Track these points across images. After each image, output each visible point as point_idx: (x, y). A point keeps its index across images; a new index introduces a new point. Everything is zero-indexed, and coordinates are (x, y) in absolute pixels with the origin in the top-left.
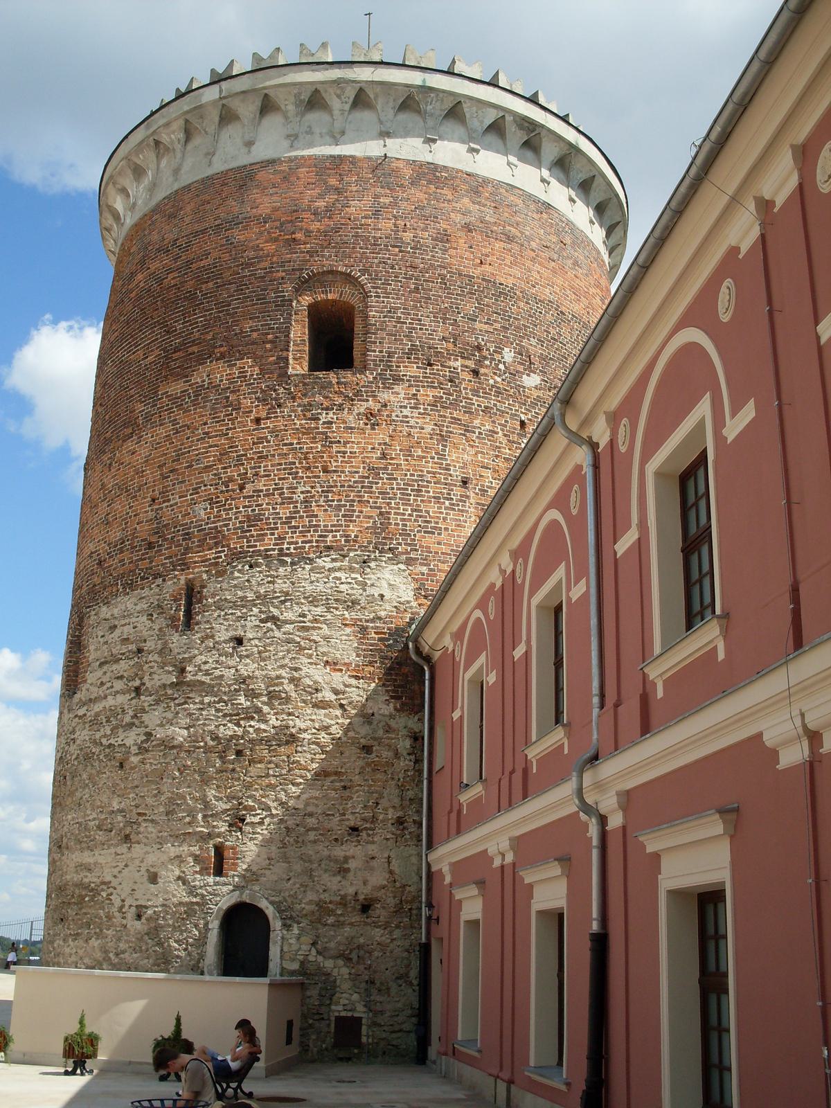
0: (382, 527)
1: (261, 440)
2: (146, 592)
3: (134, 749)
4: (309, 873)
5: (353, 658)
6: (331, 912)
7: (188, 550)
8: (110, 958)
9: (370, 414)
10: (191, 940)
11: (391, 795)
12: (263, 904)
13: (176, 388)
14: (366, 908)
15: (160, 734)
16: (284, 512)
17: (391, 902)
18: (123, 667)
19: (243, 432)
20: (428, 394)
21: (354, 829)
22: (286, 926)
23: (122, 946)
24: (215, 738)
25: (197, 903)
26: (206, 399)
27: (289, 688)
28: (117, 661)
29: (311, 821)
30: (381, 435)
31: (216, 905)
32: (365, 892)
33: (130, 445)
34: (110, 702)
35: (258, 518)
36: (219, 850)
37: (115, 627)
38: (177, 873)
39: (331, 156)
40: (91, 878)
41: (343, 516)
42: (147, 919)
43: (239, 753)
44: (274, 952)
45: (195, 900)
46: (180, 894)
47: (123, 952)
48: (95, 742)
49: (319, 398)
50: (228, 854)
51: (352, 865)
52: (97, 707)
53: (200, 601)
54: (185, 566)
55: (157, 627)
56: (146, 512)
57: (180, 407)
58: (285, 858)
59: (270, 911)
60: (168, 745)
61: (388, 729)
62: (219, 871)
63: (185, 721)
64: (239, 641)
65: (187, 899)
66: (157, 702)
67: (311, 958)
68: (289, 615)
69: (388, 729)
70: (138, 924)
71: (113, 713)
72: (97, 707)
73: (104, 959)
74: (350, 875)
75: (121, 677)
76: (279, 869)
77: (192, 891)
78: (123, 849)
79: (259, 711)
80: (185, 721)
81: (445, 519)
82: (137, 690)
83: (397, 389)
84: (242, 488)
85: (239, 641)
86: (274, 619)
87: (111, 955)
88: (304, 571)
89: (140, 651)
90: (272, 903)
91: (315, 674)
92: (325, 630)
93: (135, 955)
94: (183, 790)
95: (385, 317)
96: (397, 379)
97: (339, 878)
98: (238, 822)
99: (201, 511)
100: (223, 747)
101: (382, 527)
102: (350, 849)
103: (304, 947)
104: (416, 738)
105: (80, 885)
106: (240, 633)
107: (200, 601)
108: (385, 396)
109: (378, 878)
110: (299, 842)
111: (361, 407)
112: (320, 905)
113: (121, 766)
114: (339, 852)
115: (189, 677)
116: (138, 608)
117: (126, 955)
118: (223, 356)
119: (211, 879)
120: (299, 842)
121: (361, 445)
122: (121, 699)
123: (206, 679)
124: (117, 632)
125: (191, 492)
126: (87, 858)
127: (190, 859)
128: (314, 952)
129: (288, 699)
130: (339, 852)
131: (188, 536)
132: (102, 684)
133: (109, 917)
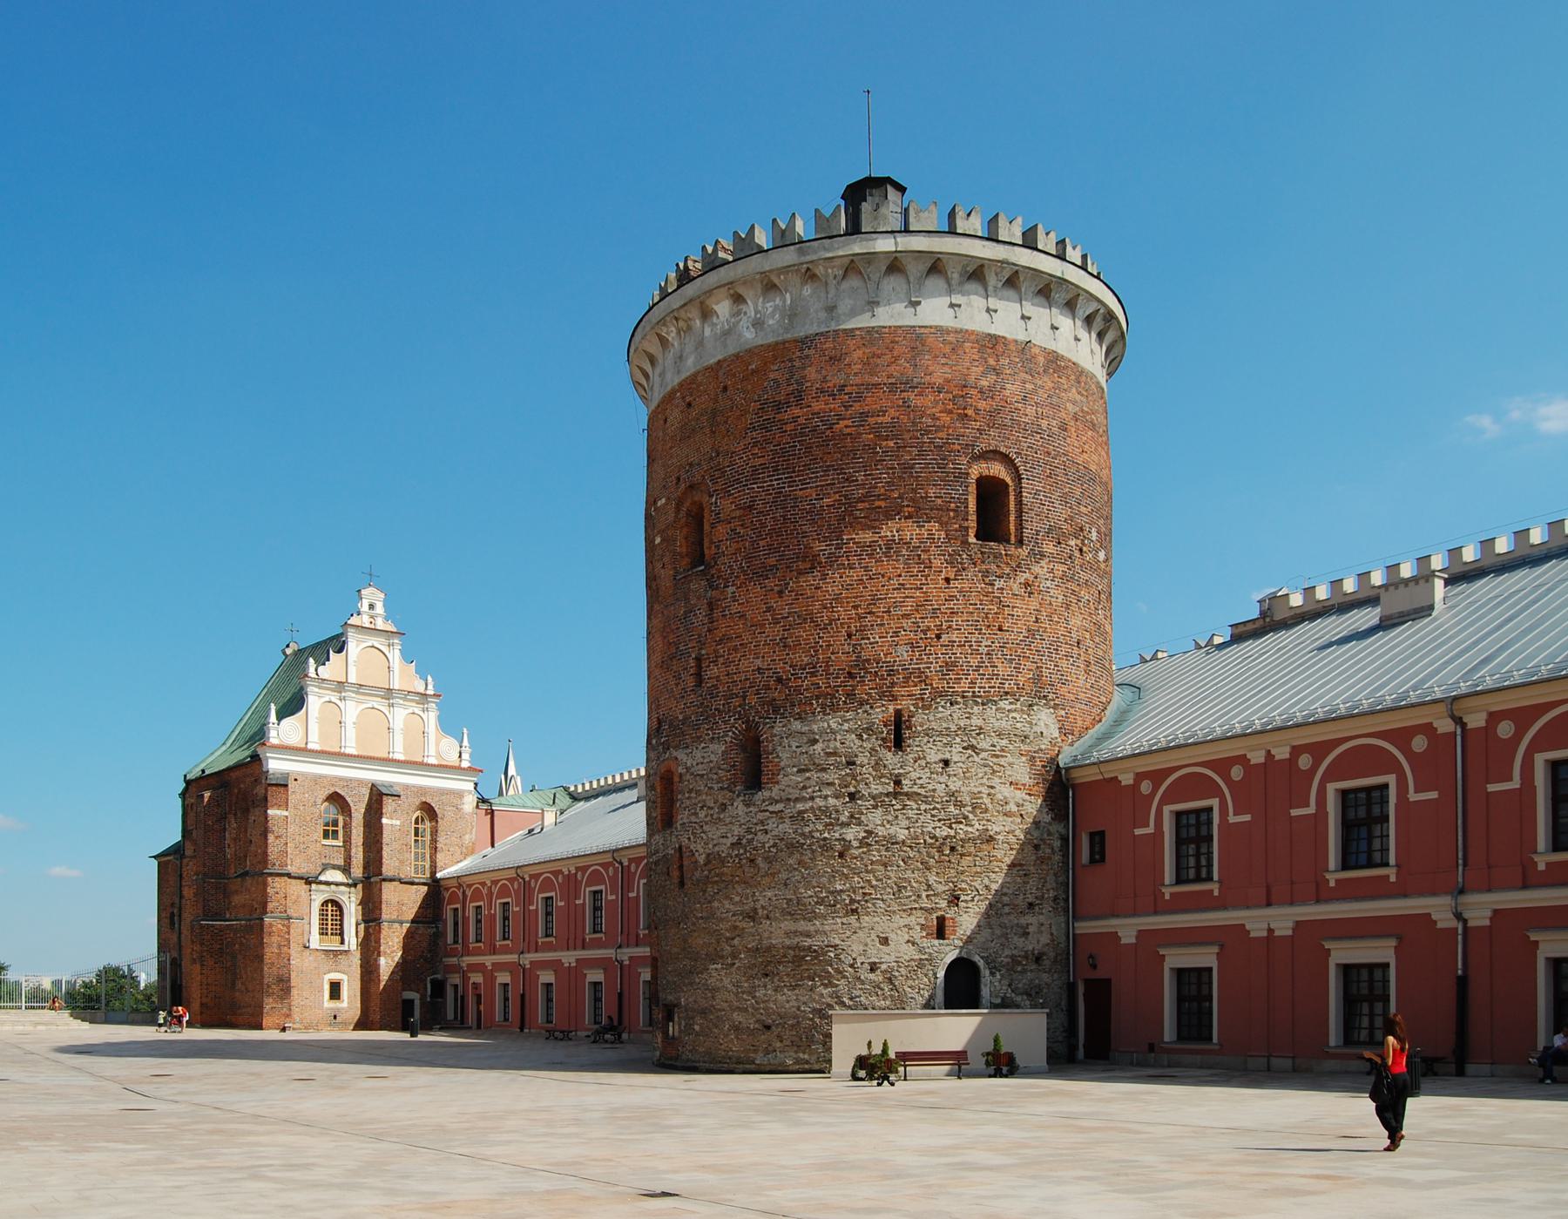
0: (1037, 679)
1: (951, 598)
2: (849, 715)
3: (855, 844)
4: (1005, 936)
5: (1026, 779)
6: (1019, 963)
7: (893, 684)
9: (1027, 584)
11: (1051, 878)
12: (977, 959)
13: (867, 536)
14: (1038, 959)
15: (881, 831)
16: (974, 662)
17: (1052, 955)
18: (831, 776)
19: (935, 588)
20: (1060, 569)
21: (1031, 905)
22: (992, 974)
23: (858, 993)
24: (934, 837)
26: (898, 553)
27: (987, 800)
28: (824, 770)
29: (1006, 899)
30: (1034, 604)
32: (1038, 947)
33: (812, 579)
34: (819, 802)
35: (954, 664)
36: (941, 921)
37: (816, 741)
38: (907, 937)
40: (815, 942)
43: (953, 849)
44: (985, 992)
46: (910, 952)
48: (803, 834)
49: (993, 567)
52: (800, 806)
53: (909, 728)
54: (894, 698)
55: (867, 745)
56: (842, 646)
57: (871, 556)
58: (990, 926)
59: (981, 963)
60: (891, 841)
61: (1049, 834)
62: (941, 933)
63: (905, 823)
64: (946, 763)
66: (875, 807)
68: (984, 745)
69: (1049, 834)
70: (872, 976)
71: (825, 811)
72: (800, 806)
75: (832, 784)
76: (986, 933)
78: (853, 918)
79: (966, 818)
80: (905, 823)
82: (852, 796)
83: (1043, 563)
84: (938, 637)
85: (946, 763)
86: (973, 747)
88: (991, 711)
89: (851, 763)
91: (1005, 791)
92: (1009, 759)
94: (909, 874)
95: (1041, 504)
96: (1043, 555)
98: (955, 900)
99: (903, 653)
100: (940, 844)
101: (1037, 679)
102: (1029, 919)
104: (1065, 839)
105: (797, 947)
106: (947, 756)
107: (909, 728)
108: (1036, 569)
109: (1045, 939)
110: (999, 915)
111: (1023, 577)
112: (1013, 957)
113: (841, 855)
114: (1023, 921)
115: (906, 789)
116: (846, 726)
118: (909, 517)
119: (936, 942)
120: (999, 915)
121: (1024, 608)
122: (832, 801)
123: (922, 791)
124: (818, 747)
126: (803, 926)
129: (986, 811)
131: (891, 673)
132: (805, 788)
133: (838, 971)
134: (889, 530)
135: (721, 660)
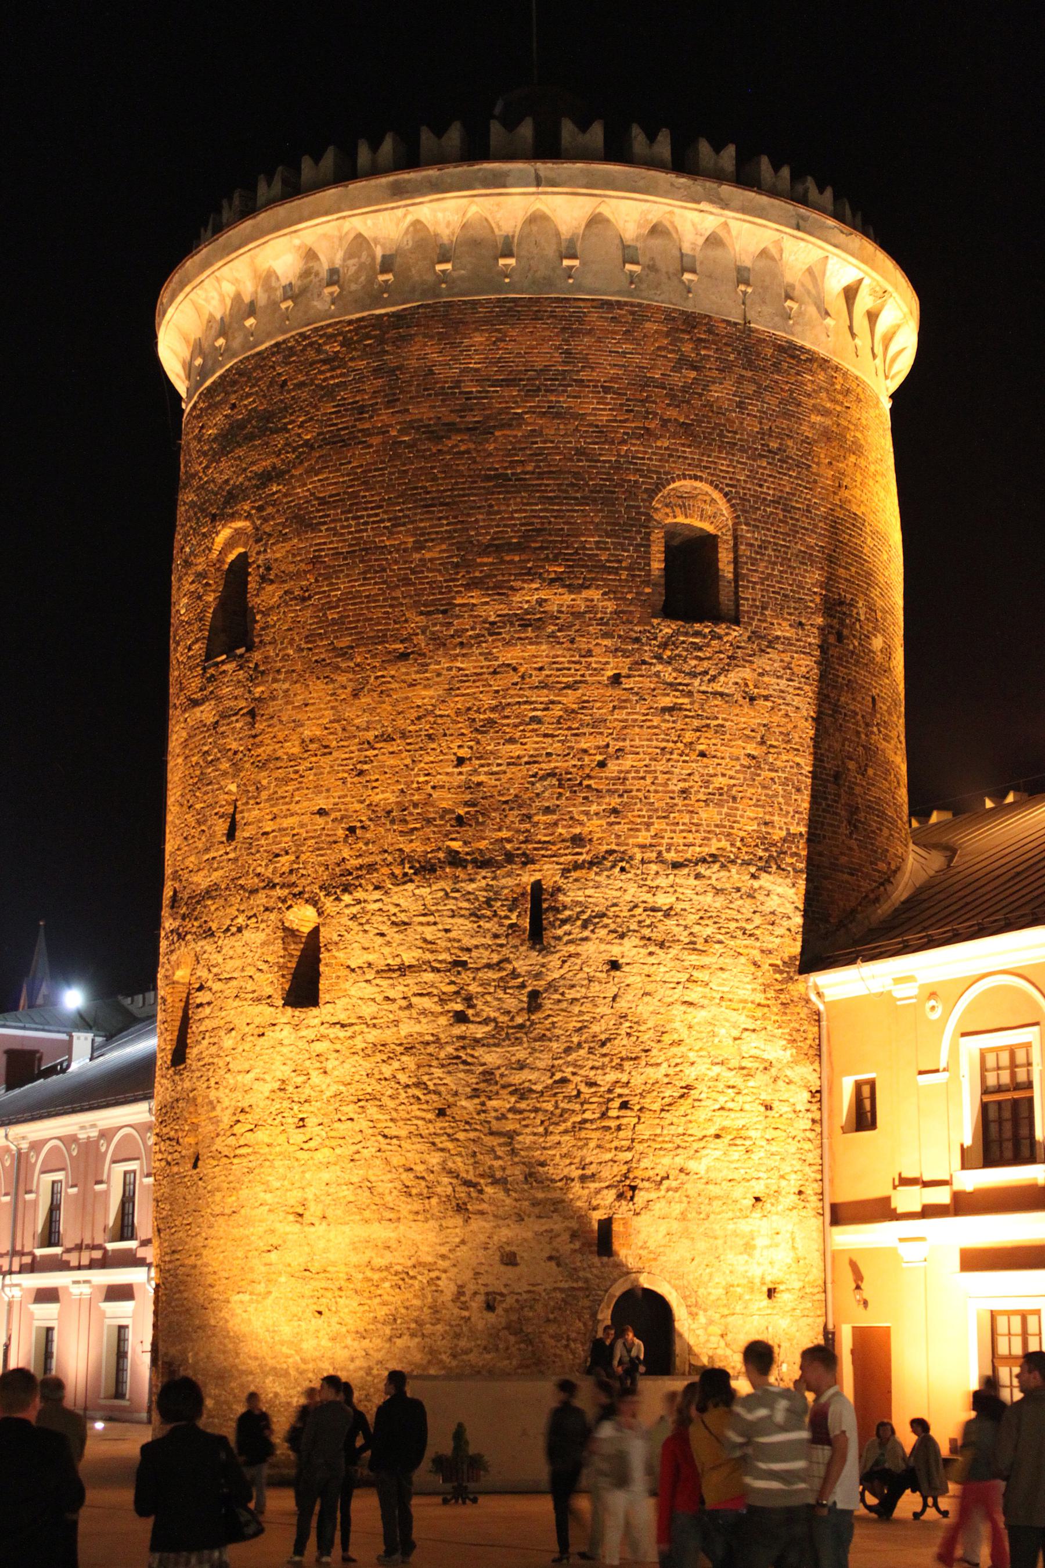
8: (441, 1361)
10: (573, 1335)
25: (580, 1289)
31: (606, 1291)
39: (683, 312)
41: (727, 815)
42: (506, 1310)
45: (575, 1285)
47: (466, 1352)
50: (616, 1227)
51: (759, 1242)
65: (566, 1285)
67: (720, 1352)
70: (491, 1317)
73: (429, 1362)
74: (757, 1253)
77: (573, 1273)
81: (823, 824)
84: (602, 764)
87: (444, 1357)
90: (676, 1288)
93: (488, 1356)
97: (745, 1257)
103: (712, 1338)
108: (761, 662)
117: (472, 1357)
119: (596, 1260)
125: (526, 759)
127: (566, 1237)
128: (722, 1344)
130: (744, 1226)
134: (527, 596)
135: (264, 795)
